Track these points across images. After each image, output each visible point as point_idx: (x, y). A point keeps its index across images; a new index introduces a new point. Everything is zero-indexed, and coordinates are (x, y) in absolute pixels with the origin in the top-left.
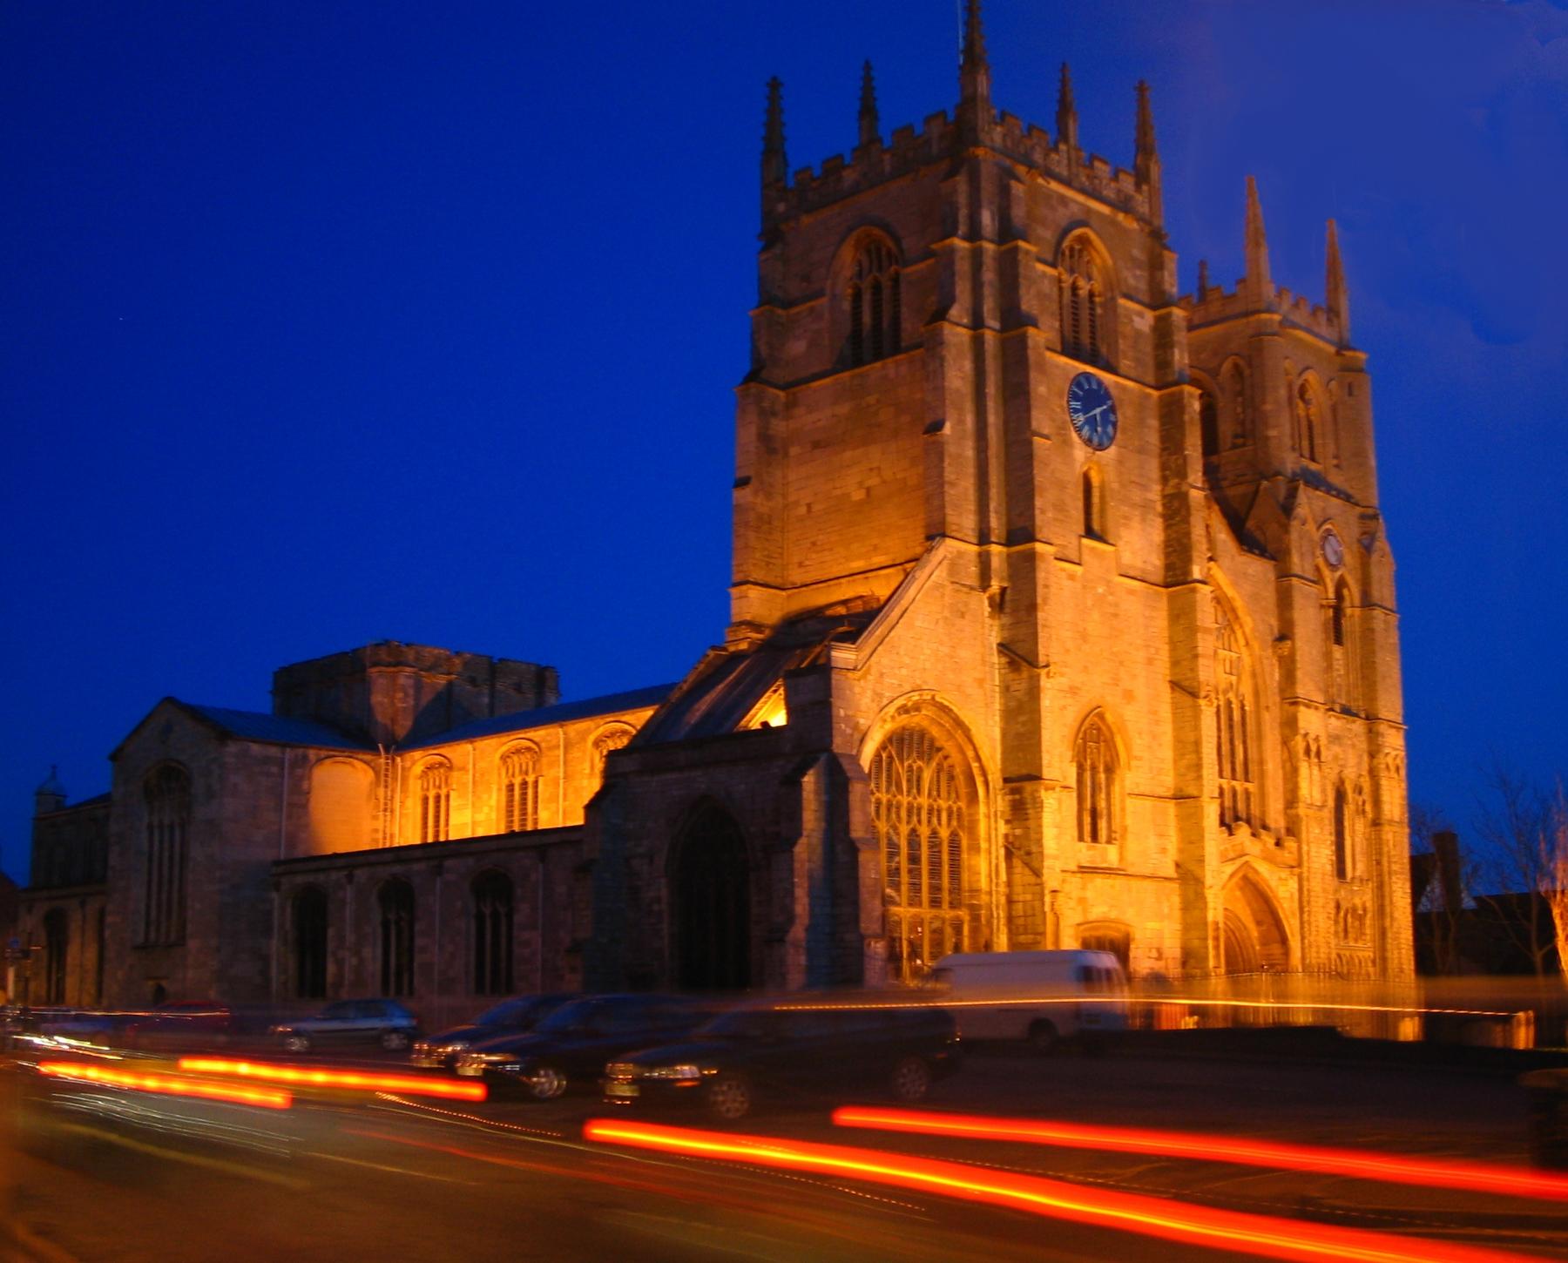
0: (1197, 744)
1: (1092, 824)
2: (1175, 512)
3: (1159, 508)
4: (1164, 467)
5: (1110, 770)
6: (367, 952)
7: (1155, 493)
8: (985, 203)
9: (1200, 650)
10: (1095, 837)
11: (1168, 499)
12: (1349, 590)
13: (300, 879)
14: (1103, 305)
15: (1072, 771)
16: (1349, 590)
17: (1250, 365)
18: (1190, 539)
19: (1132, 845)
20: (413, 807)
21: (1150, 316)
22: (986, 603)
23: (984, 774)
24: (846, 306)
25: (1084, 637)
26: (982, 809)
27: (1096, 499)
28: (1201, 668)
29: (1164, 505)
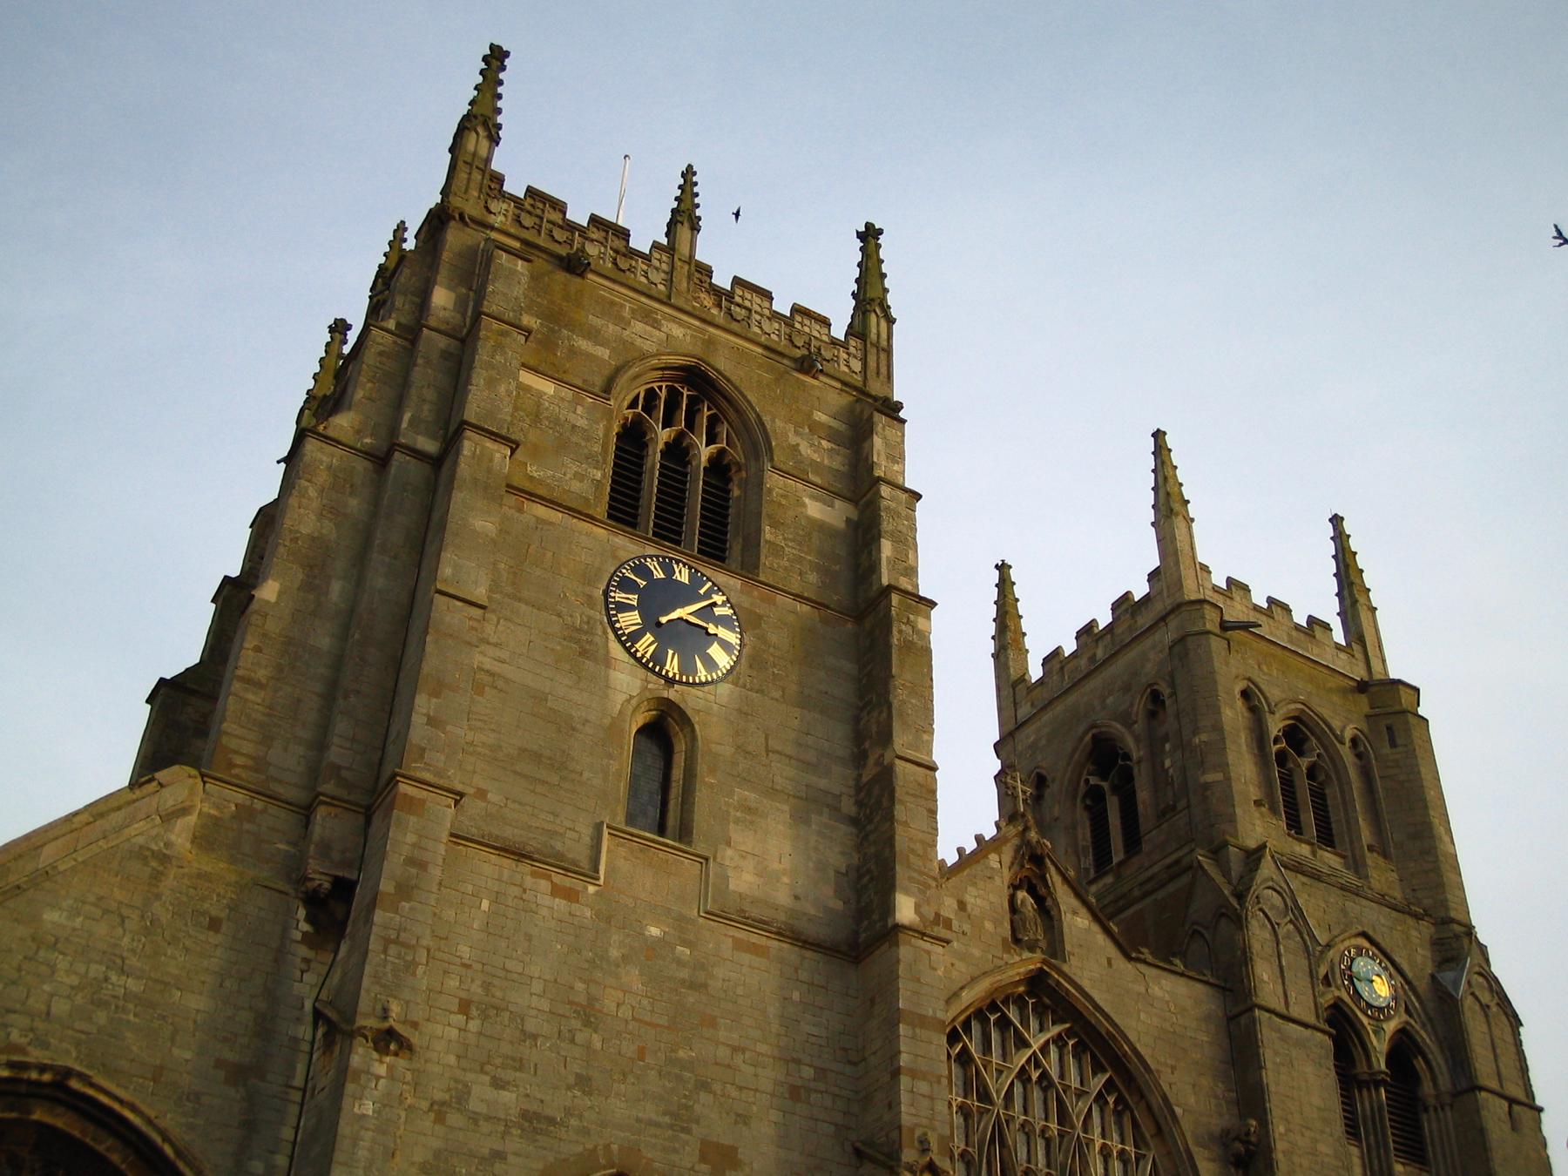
3: (848, 806)
8: (443, 274)
9: (904, 1060)
12: (1427, 1062)
14: (744, 485)
16: (1427, 1062)
17: (1172, 685)
18: (892, 846)
22: (302, 913)
25: (589, 1015)
28: (904, 1097)
29: (860, 804)
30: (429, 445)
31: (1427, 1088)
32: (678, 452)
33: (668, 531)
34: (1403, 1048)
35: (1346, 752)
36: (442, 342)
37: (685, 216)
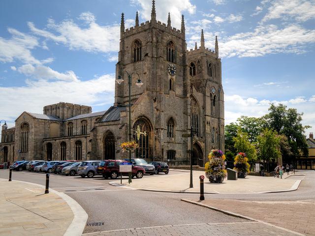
0: (187, 123)
1: (170, 134)
2: (185, 86)
4: (184, 78)
5: (173, 126)
6: (58, 153)
7: (182, 83)
10: (170, 137)
11: (184, 84)
13: (47, 142)
15: (167, 127)
19: (176, 138)
20: (67, 130)
21: (182, 54)
23: (152, 126)
24: (133, 52)
25: (169, 105)
26: (152, 132)
27: (172, 84)
30: (156, 56)
31: (216, 100)
32: (170, 50)
33: (173, 62)
34: (215, 96)
35: (214, 67)
36: (155, 44)
37: (169, 21)
